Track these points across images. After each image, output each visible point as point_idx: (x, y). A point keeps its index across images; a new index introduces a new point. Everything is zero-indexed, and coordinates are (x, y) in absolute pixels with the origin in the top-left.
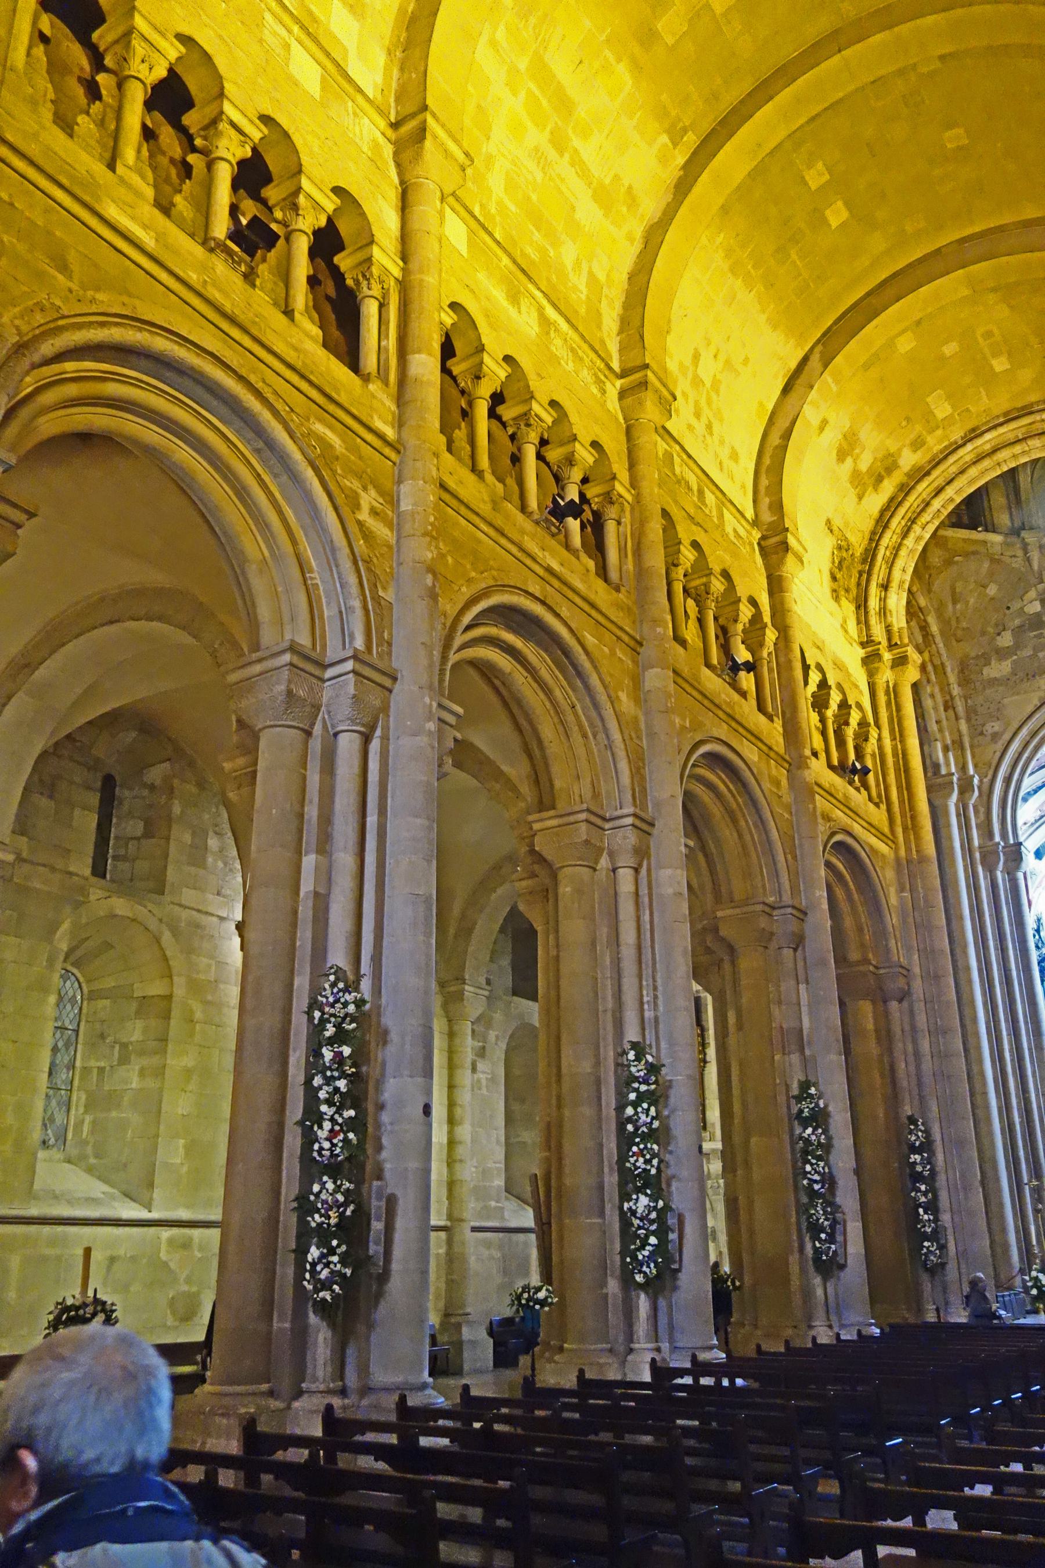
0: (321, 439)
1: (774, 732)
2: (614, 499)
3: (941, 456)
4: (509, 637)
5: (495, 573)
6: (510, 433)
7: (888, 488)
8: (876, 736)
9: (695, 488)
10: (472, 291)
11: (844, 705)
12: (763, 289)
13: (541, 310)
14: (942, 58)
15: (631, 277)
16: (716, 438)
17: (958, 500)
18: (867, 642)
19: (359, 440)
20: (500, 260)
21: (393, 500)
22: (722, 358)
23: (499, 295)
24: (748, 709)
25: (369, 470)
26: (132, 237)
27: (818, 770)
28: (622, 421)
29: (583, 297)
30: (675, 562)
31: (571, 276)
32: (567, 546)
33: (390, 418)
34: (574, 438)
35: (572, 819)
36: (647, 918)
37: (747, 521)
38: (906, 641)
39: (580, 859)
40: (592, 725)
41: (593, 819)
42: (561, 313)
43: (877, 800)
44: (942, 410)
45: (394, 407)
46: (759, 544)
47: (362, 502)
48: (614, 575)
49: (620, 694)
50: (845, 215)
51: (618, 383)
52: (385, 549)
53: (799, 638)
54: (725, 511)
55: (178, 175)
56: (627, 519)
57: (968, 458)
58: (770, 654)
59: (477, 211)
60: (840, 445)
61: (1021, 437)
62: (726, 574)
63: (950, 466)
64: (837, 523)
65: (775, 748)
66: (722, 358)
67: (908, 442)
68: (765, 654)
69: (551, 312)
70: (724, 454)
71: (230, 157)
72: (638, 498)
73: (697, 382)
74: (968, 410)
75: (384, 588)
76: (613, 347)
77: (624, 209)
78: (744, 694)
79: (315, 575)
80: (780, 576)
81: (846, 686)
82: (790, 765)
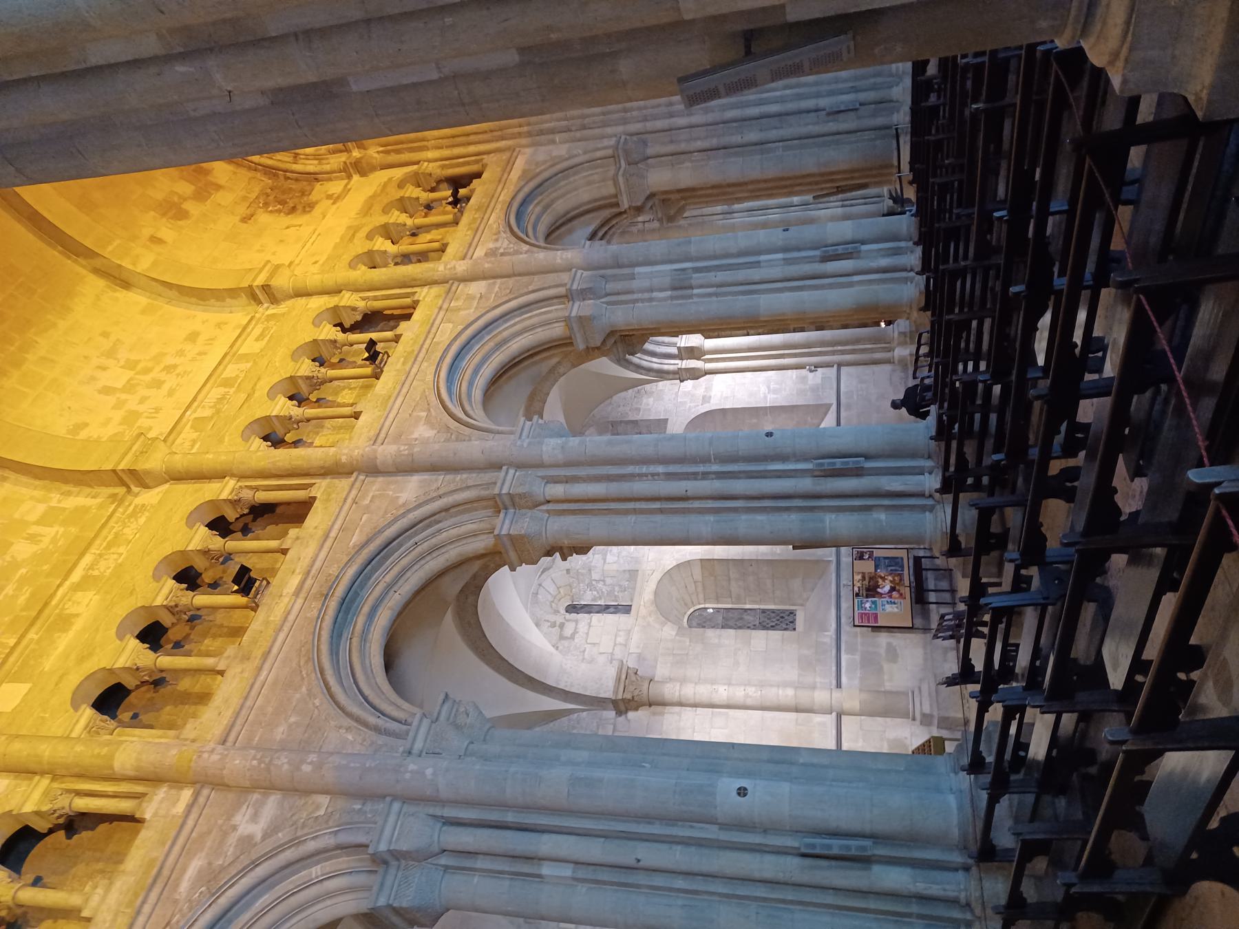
0: (193, 888)
5: (302, 663)
9: (222, 390)
10: (61, 677)
13: (77, 587)
16: (177, 361)
19: (194, 834)
23: (64, 641)
25: (220, 822)
29: (62, 529)
31: (43, 545)
33: (173, 792)
49: (401, 501)
58: (363, 299)
60: (172, 218)
64: (242, 210)
69: (76, 576)
73: (129, 387)
75: (318, 807)
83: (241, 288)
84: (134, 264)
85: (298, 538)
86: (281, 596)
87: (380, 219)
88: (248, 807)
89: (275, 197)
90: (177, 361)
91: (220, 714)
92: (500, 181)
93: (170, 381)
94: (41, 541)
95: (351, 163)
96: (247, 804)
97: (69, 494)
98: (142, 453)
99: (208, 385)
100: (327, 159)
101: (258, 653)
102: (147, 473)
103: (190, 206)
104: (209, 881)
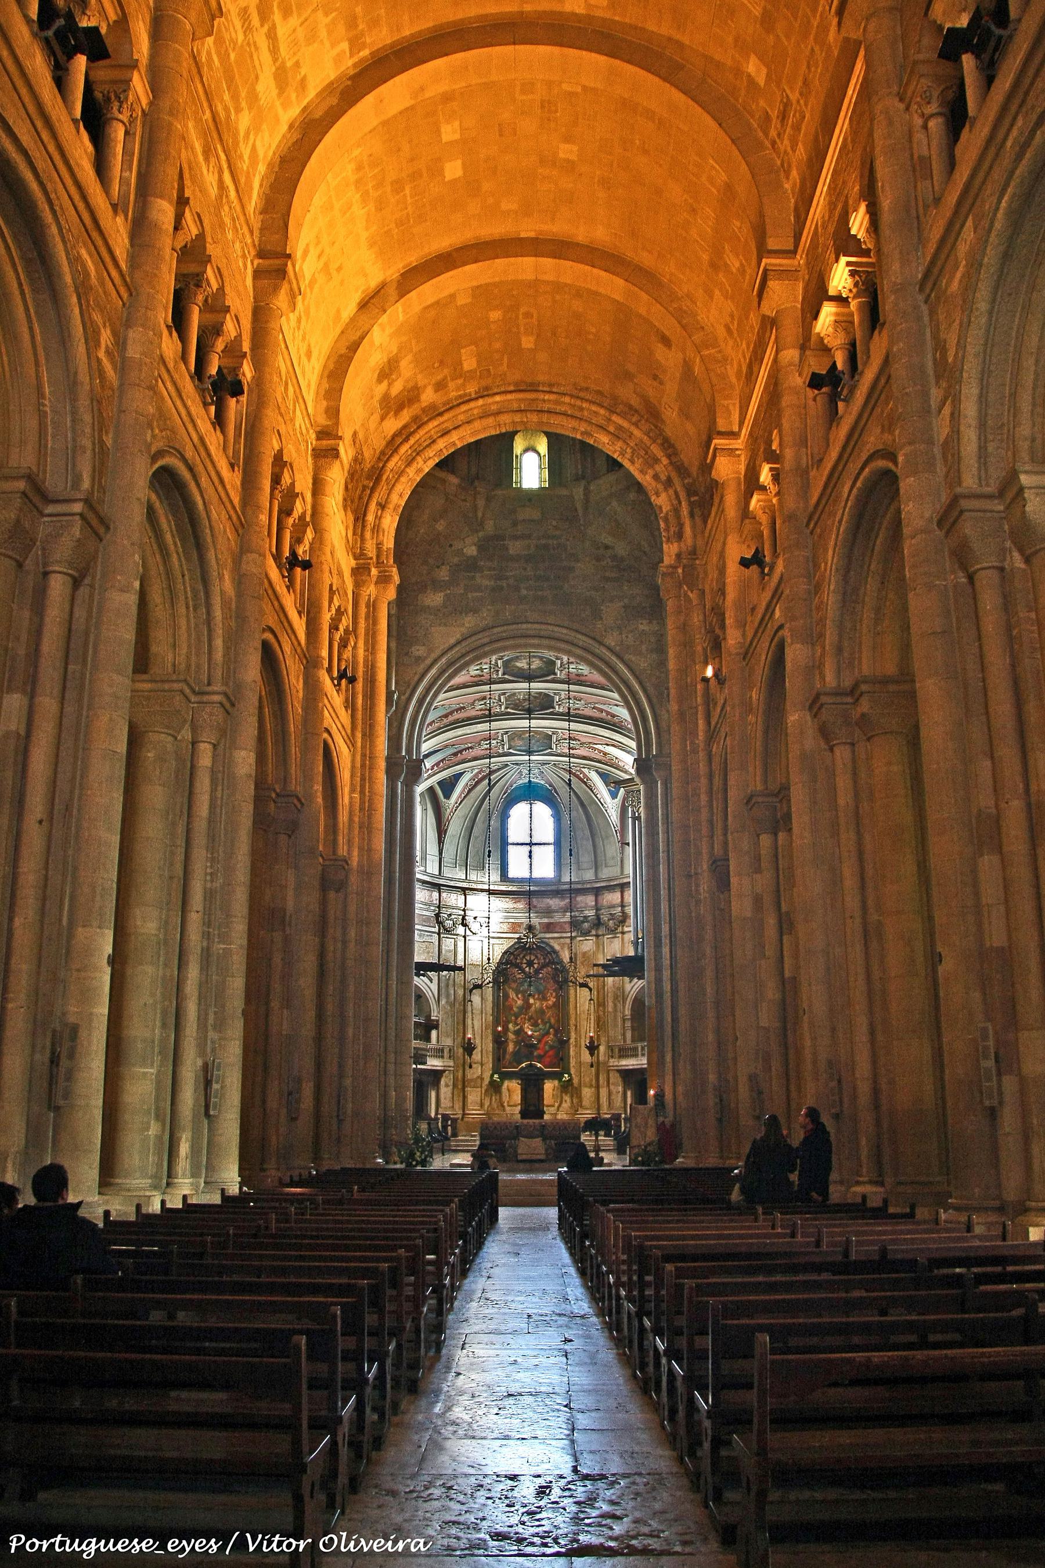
7: (406, 416)
11: (338, 610)
12: (373, 209)
14: (584, 88)
17: (459, 445)
20: (204, 113)
22: (324, 259)
38: (392, 561)
39: (168, 727)
44: (469, 363)
50: (459, 173)
51: (256, 262)
57: (475, 412)
63: (460, 414)
66: (324, 259)
67: (433, 381)
69: (227, 177)
70: (303, 350)
74: (488, 370)
77: (294, 96)
79: (47, 402)
83: (337, 424)
84: (381, 325)
90: (301, 332)
93: (293, 323)
95: (369, 564)
97: (261, 185)
99: (289, 364)
102: (276, 289)
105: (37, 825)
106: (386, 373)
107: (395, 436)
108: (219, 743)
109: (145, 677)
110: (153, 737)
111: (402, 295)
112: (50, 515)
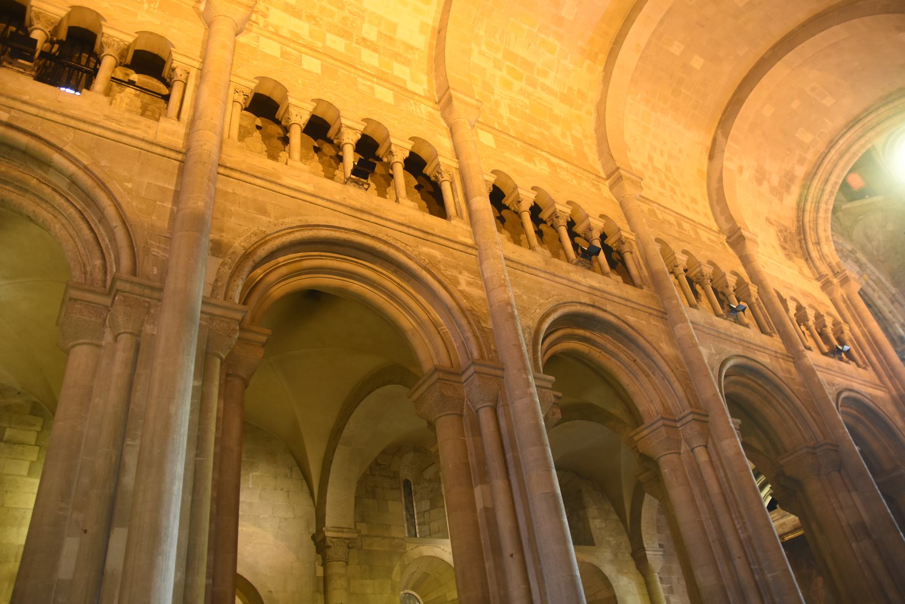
1: (775, 342)
2: (624, 240)
3: (819, 163)
4: (581, 332)
5: (555, 297)
6: (549, 225)
7: (796, 190)
8: (848, 328)
9: (675, 223)
11: (818, 316)
13: (548, 161)
15: (596, 130)
18: (820, 277)
19: (451, 250)
21: (480, 274)
23: (520, 160)
24: (753, 334)
25: (461, 263)
26: (299, 189)
27: (814, 357)
28: (616, 201)
29: (572, 148)
30: (676, 264)
32: (603, 273)
33: (468, 234)
34: (587, 216)
35: (655, 426)
36: (722, 474)
37: (716, 232)
39: (668, 450)
40: (650, 368)
41: (667, 422)
42: (560, 158)
43: (864, 366)
45: (469, 228)
46: (727, 242)
47: (460, 280)
48: (638, 281)
49: (661, 345)
51: (607, 183)
52: (481, 301)
53: (772, 285)
54: (697, 229)
55: (335, 162)
56: (635, 249)
57: (835, 157)
58: (757, 299)
59: (496, 126)
60: (756, 176)
61: (861, 135)
62: (711, 263)
65: (779, 351)
68: (754, 300)
69: (554, 160)
71: (350, 141)
72: (638, 237)
73: (656, 170)
76: (598, 167)
78: (747, 326)
80: (746, 255)
81: (816, 305)
82: (793, 358)
85: (618, 282)
86: (585, 278)
87: (804, 303)
88: (473, 278)
89: (787, 236)
91: (514, 252)
92: (865, 381)
94: (563, 139)
96: (475, 278)
98: (633, 182)
99: (674, 214)
100: (824, 264)
101: (551, 269)
103: (765, 187)
104: (431, 263)
105: (510, 558)
106: (761, 177)
107: (798, 205)
108: (707, 443)
109: (643, 427)
110: (662, 460)
111: (727, 138)
112: (465, 382)
